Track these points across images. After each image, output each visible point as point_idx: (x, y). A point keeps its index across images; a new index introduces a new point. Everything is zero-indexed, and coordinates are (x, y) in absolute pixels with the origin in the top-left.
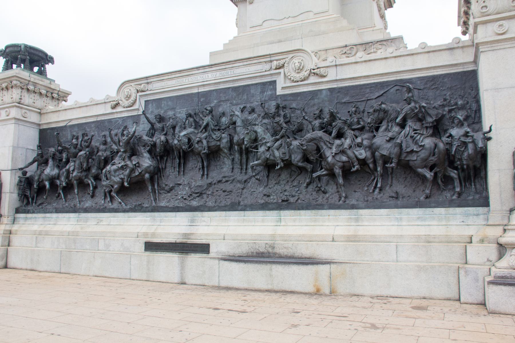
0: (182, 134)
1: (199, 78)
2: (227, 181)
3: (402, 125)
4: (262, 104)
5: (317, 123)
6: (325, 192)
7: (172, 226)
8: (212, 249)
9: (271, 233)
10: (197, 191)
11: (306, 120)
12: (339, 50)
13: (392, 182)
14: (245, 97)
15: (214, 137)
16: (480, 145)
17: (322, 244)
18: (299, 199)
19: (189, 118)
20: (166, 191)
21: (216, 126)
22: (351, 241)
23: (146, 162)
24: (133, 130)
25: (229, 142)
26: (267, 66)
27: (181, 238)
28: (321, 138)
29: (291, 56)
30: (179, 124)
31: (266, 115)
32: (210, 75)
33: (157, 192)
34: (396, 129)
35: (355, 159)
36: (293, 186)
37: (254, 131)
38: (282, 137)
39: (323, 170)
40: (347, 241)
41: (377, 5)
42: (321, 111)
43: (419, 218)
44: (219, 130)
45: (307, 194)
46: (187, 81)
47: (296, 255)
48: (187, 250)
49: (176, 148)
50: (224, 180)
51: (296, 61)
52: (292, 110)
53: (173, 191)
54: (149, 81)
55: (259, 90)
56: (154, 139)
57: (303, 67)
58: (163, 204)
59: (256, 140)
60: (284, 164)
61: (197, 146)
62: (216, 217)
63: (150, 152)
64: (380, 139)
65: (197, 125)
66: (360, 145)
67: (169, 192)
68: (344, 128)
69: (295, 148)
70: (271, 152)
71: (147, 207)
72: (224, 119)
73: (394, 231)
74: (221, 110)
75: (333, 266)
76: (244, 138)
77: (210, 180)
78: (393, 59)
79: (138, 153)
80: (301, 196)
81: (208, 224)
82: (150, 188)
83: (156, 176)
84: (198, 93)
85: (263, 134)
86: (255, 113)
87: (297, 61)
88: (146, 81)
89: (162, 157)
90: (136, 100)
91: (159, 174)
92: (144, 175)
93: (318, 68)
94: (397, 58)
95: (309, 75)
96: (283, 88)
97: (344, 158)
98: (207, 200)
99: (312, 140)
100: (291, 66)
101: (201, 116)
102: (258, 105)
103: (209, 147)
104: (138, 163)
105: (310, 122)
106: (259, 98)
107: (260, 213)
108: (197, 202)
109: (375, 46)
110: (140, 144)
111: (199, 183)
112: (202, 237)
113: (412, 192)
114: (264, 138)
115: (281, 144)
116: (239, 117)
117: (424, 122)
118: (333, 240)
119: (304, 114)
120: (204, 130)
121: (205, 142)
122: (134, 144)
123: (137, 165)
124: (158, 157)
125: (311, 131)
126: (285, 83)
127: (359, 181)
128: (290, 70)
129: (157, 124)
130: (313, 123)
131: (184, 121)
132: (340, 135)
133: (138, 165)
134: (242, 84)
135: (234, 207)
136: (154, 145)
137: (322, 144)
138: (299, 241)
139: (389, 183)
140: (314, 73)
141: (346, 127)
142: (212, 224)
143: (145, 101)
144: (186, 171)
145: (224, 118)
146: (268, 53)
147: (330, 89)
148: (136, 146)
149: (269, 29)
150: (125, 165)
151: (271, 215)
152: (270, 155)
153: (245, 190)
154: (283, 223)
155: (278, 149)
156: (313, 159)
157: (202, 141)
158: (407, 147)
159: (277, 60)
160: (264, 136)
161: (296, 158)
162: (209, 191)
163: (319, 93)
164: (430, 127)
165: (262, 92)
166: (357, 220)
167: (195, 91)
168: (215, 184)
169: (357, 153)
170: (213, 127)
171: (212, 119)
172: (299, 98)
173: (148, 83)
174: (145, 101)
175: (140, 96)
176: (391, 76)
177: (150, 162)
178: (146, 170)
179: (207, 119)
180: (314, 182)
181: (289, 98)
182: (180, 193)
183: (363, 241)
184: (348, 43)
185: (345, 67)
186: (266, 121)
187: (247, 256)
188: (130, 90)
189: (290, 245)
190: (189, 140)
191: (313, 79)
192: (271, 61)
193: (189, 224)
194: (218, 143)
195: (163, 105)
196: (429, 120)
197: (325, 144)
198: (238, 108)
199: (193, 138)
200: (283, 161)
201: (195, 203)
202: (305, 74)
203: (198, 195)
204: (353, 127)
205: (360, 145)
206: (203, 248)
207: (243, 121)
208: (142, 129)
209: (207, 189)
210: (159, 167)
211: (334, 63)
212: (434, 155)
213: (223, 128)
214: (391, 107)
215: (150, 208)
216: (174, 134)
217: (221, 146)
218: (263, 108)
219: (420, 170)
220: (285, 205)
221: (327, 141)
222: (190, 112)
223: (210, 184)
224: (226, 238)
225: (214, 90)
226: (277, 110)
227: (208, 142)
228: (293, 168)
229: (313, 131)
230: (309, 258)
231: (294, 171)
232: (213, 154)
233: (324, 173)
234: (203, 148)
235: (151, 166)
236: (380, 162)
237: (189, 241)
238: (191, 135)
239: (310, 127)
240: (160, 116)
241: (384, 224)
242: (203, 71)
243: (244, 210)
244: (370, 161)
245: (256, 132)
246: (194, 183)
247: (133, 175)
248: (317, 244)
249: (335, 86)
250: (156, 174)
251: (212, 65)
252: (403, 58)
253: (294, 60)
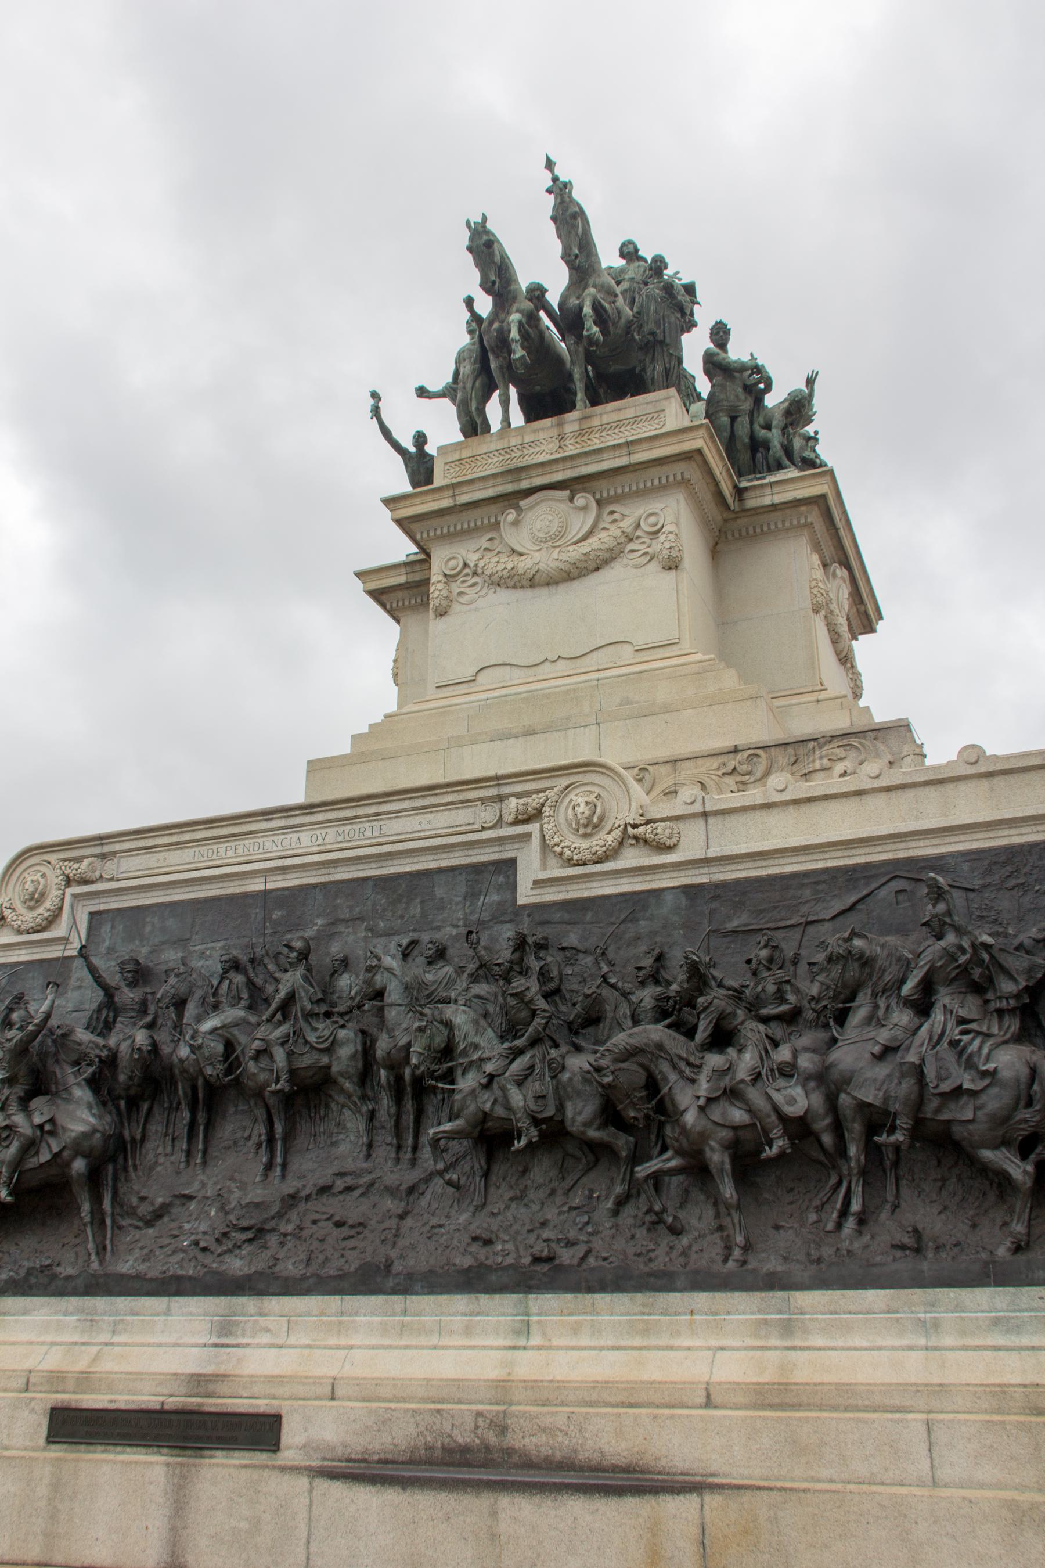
0: (207, 1026)
1: (269, 846)
2: (349, 1189)
3: (922, 1007)
4: (470, 932)
5: (646, 996)
6: (676, 1231)
7: (154, 1347)
8: (292, 1435)
9: (494, 1374)
10: (245, 1223)
11: (613, 986)
12: (714, 763)
13: (898, 1196)
14: (416, 910)
15: (312, 1038)
17: (672, 1416)
18: (589, 1252)
19: (232, 974)
20: (141, 1219)
21: (319, 1001)
22: (772, 1407)
23: (80, 1116)
24: (44, 1008)
25: (360, 1056)
26: (488, 815)
27: (183, 1390)
28: (660, 1046)
29: (564, 782)
30: (199, 993)
31: (484, 971)
32: (305, 837)
33: (108, 1221)
34: (903, 1017)
35: (774, 1117)
36: (571, 1209)
37: (441, 1022)
38: (534, 1043)
39: (669, 1154)
40: (755, 1406)
41: (828, 625)
42: (660, 958)
43: (996, 1322)
44: (328, 1015)
45: (617, 1238)
46: (230, 853)
47: (582, 1456)
48: (199, 1439)
49: (185, 1071)
50: (340, 1184)
51: (580, 800)
52: (568, 954)
53: (166, 1219)
54: (106, 849)
55: (462, 889)
56: (112, 1042)
57: (601, 819)
58: (126, 1266)
59: (448, 1051)
60: (542, 1134)
61: (252, 1067)
62: (309, 1314)
63: (94, 1083)
64: (852, 1053)
65: (256, 999)
66: (787, 1071)
67: (149, 1224)
68: (734, 1014)
69: (578, 1078)
70: (498, 1093)
71: (69, 1278)
72: (345, 981)
73: (914, 1368)
74: (336, 948)
75: (712, 1500)
76: (409, 1045)
77: (290, 1186)
78: (882, 797)
79: (53, 1088)
80: (597, 1243)
81: (279, 1341)
82: (86, 1207)
83: (110, 1167)
84: (265, 892)
85: (472, 1033)
86: (448, 963)
87: (581, 800)
88: (98, 850)
89: (133, 1103)
90: (61, 909)
91: (121, 1160)
92: (68, 1164)
93: (648, 822)
94: (893, 794)
95: (621, 843)
96: (537, 883)
97: (738, 1115)
98: (280, 1256)
99: (631, 1053)
100: (565, 813)
101: (271, 967)
102: (456, 938)
103: (292, 1072)
104: (52, 1121)
105: (625, 995)
106: (460, 915)
107: (460, 1302)
108: (245, 1264)
109: (825, 750)
110: (62, 1056)
111: (257, 1194)
112: (256, 1390)
113: (966, 1229)
114: (476, 1047)
115: (532, 1067)
116: (395, 974)
117: (990, 995)
118: (709, 1403)
119: (605, 969)
120: (279, 1016)
121: (280, 1054)
122: (43, 1055)
123: (47, 1127)
124: (122, 1103)
125: (629, 1023)
126: (544, 866)
127: (792, 1190)
128: (558, 825)
129: (126, 990)
130: (634, 998)
131: (215, 983)
132: (723, 1038)
133: (50, 1129)
134: (407, 869)
135: (370, 1279)
136: (111, 1061)
137: (665, 1067)
138: (591, 1404)
139: (890, 1198)
140: (636, 838)
141: (739, 1012)
142: (292, 1341)
143: (91, 914)
144: (213, 1152)
145: (346, 976)
146: (491, 773)
147: (686, 889)
148: (50, 1061)
149: (497, 693)
150: (7, 1127)
151: (497, 1311)
152: (495, 1101)
153: (409, 1222)
154: (535, 1340)
155: (520, 1084)
156: (635, 1114)
157: (273, 1054)
158: (940, 1079)
159: (518, 795)
160: (476, 1040)
161: (580, 1113)
162: (289, 1221)
163: (653, 901)
164: (1012, 1011)
165: (472, 895)
166: (787, 1328)
167: (256, 886)
168: (308, 1197)
169: (777, 1097)
170: (309, 1007)
171: (306, 978)
172: (589, 916)
173: (103, 856)
174: (92, 914)
175: (75, 896)
176: (879, 849)
177: (92, 1120)
178: (78, 1148)
179: (292, 979)
180: (639, 1194)
181: (557, 916)
182: (187, 1226)
183: (809, 1407)
184: (741, 741)
185: (733, 818)
186: (482, 989)
187: (411, 1462)
188: (44, 876)
189: (561, 1421)
190: (229, 1046)
191: (632, 858)
192: (501, 799)
193: (214, 1340)
194: (325, 1060)
195: (148, 928)
196: (1008, 987)
197: (675, 1067)
198: (392, 946)
199: (243, 1039)
200: (536, 1122)
201: (236, 1265)
202: (606, 838)
203: (250, 1235)
204: (764, 1012)
205: (787, 1071)
206: (259, 1432)
207: (407, 988)
208: (73, 1006)
209: (280, 1215)
210: (121, 1135)
211: (698, 808)
212: (1029, 1104)
213: (341, 1009)
214: (883, 946)
215: (80, 1282)
216: (178, 1026)
217: (335, 1069)
218: (474, 946)
219: (987, 1155)
220: (544, 1273)
221: (680, 1058)
222: (235, 952)
223: (293, 1197)
224: (339, 1392)
225: (315, 886)
226: (517, 955)
227: (290, 1054)
228: (571, 1148)
229: (636, 1022)
230: (627, 1469)
231: (573, 1156)
232: (307, 1095)
233: (673, 1163)
234: (272, 1073)
235: (95, 1131)
236: (855, 1129)
237: (211, 1404)
238: (235, 1031)
239: (625, 1009)
240: (138, 963)
241: (880, 1342)
242: (282, 823)
243: (404, 1289)
244: (822, 1124)
245: (448, 1025)
246: (237, 1194)
247: (32, 1162)
248: (655, 1417)
249: (704, 879)
250: (110, 1158)
251: (312, 806)
252: (910, 794)
253: (572, 796)
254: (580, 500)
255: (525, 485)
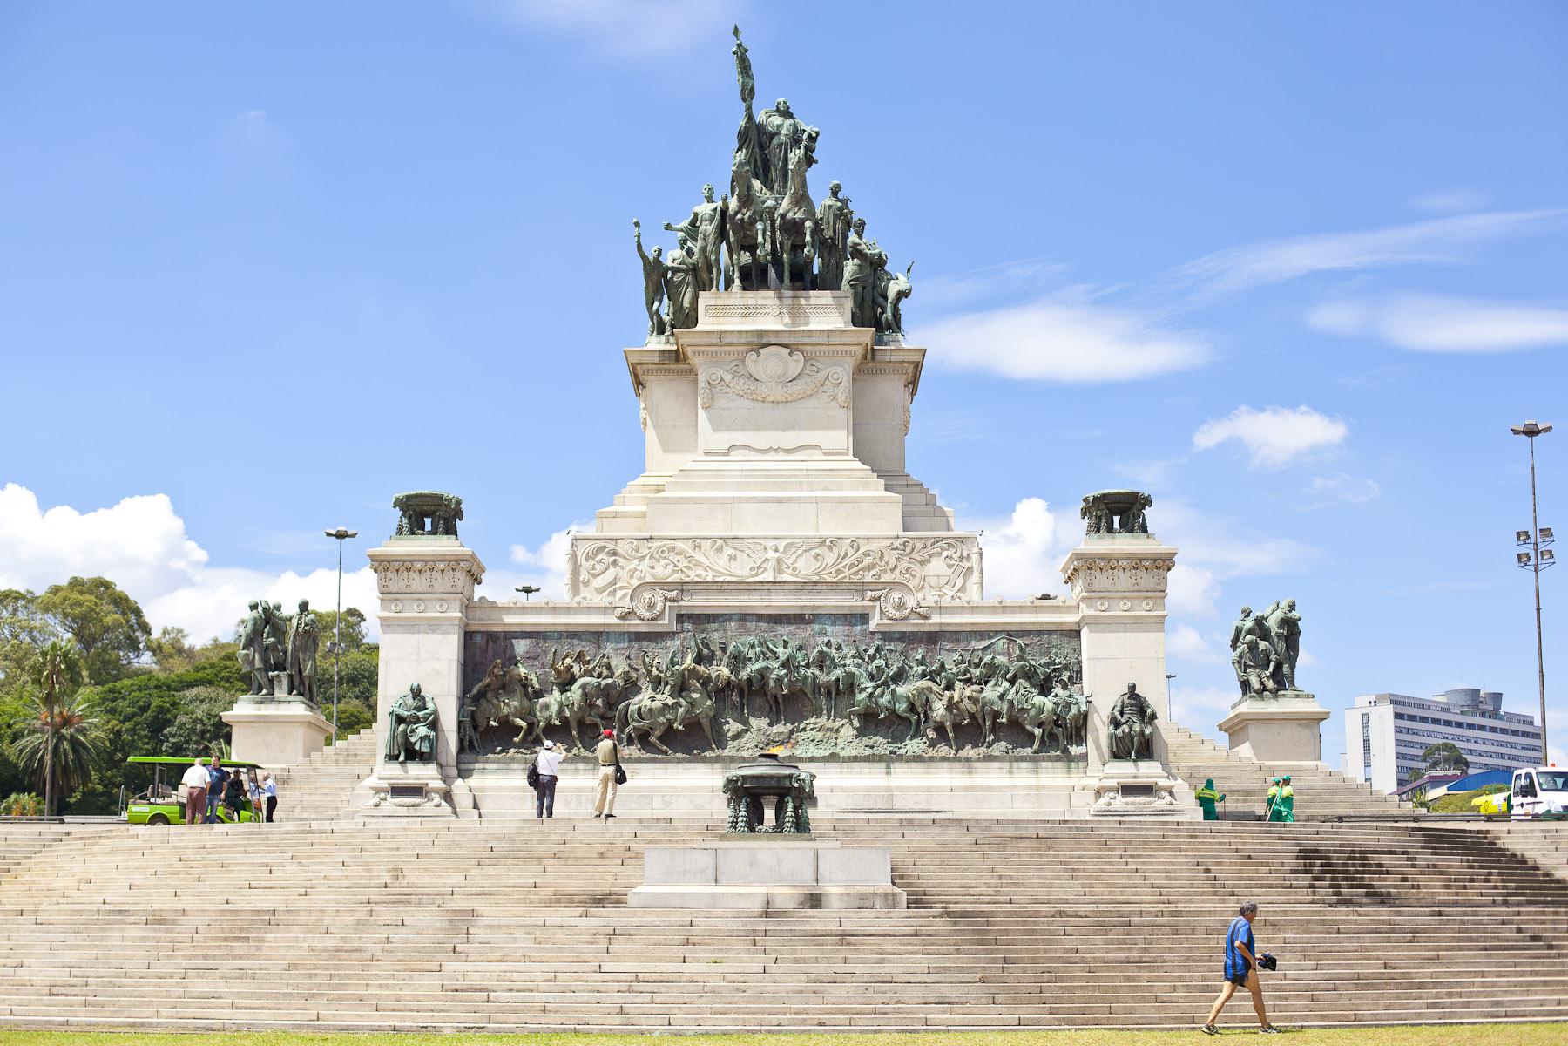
3: (1012, 682)
16: (1083, 708)
34: (1006, 684)
64: (991, 692)
73: (1007, 782)
161: (901, 707)
254: (798, 356)
255: (765, 341)
